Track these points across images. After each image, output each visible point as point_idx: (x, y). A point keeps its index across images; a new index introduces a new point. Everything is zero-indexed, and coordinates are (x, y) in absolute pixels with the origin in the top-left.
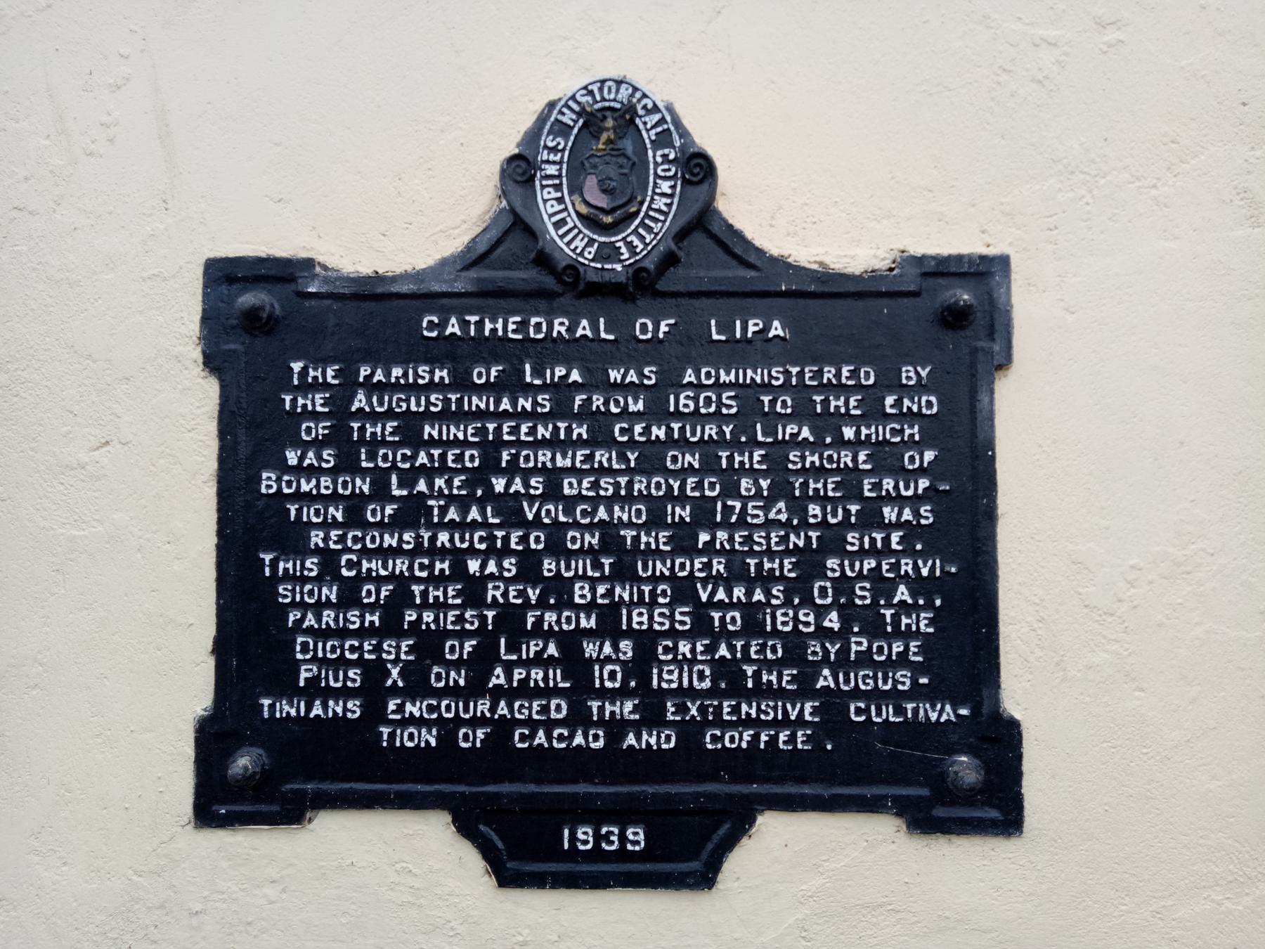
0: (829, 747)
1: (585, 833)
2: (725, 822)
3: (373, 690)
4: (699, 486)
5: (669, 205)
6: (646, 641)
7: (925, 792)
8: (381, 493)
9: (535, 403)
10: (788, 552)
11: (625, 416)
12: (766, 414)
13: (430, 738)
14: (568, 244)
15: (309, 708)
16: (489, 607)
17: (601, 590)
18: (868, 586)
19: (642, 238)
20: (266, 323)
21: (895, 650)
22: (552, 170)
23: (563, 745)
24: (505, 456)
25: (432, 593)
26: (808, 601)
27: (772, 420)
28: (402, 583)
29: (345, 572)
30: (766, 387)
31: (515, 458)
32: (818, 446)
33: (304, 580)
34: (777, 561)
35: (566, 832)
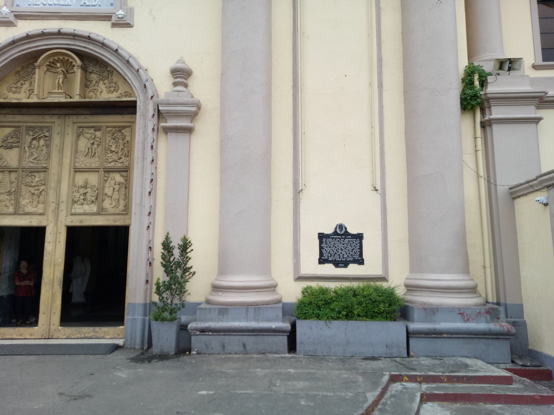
3: (328, 257)
20: (322, 237)
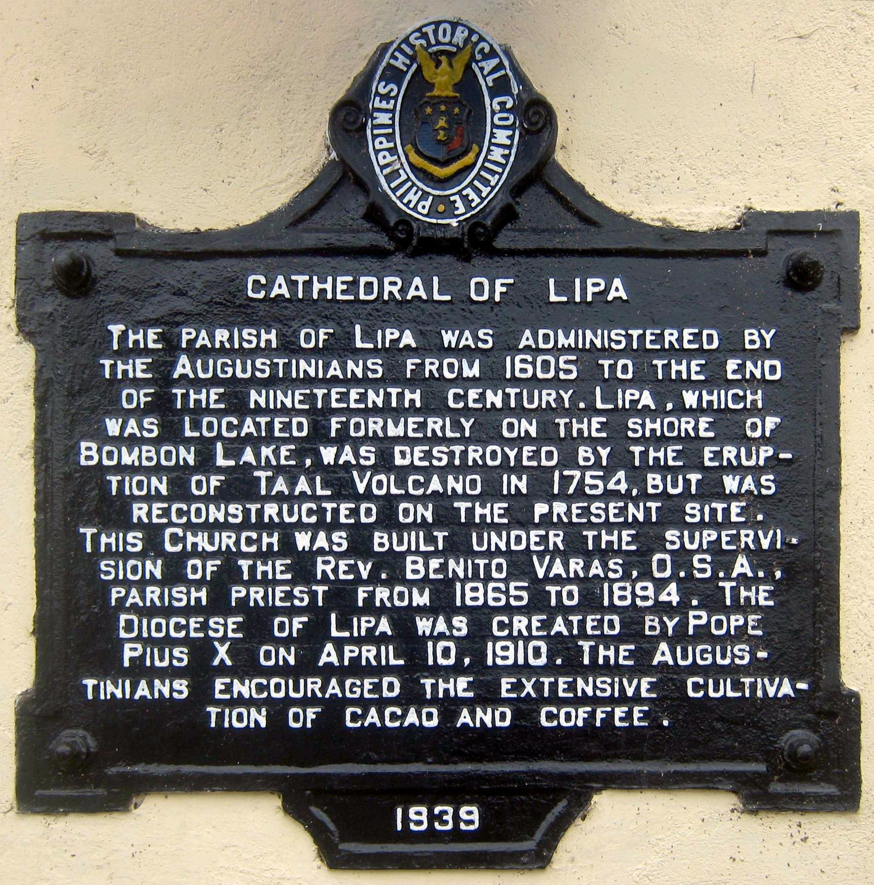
0: (666, 723)
1: (418, 814)
2: (560, 800)
3: (201, 669)
4: (536, 455)
6: (479, 618)
7: (762, 768)
9: (366, 368)
10: (626, 525)
11: (460, 382)
12: (606, 380)
15: (134, 688)
17: (434, 563)
18: (708, 558)
19: (478, 192)
21: (733, 624)
22: (383, 118)
23: (397, 724)
24: (335, 424)
25: (260, 568)
26: (645, 574)
27: (612, 385)
28: (229, 558)
31: (345, 425)
32: (659, 412)
33: (126, 556)
34: (616, 533)
35: (399, 811)
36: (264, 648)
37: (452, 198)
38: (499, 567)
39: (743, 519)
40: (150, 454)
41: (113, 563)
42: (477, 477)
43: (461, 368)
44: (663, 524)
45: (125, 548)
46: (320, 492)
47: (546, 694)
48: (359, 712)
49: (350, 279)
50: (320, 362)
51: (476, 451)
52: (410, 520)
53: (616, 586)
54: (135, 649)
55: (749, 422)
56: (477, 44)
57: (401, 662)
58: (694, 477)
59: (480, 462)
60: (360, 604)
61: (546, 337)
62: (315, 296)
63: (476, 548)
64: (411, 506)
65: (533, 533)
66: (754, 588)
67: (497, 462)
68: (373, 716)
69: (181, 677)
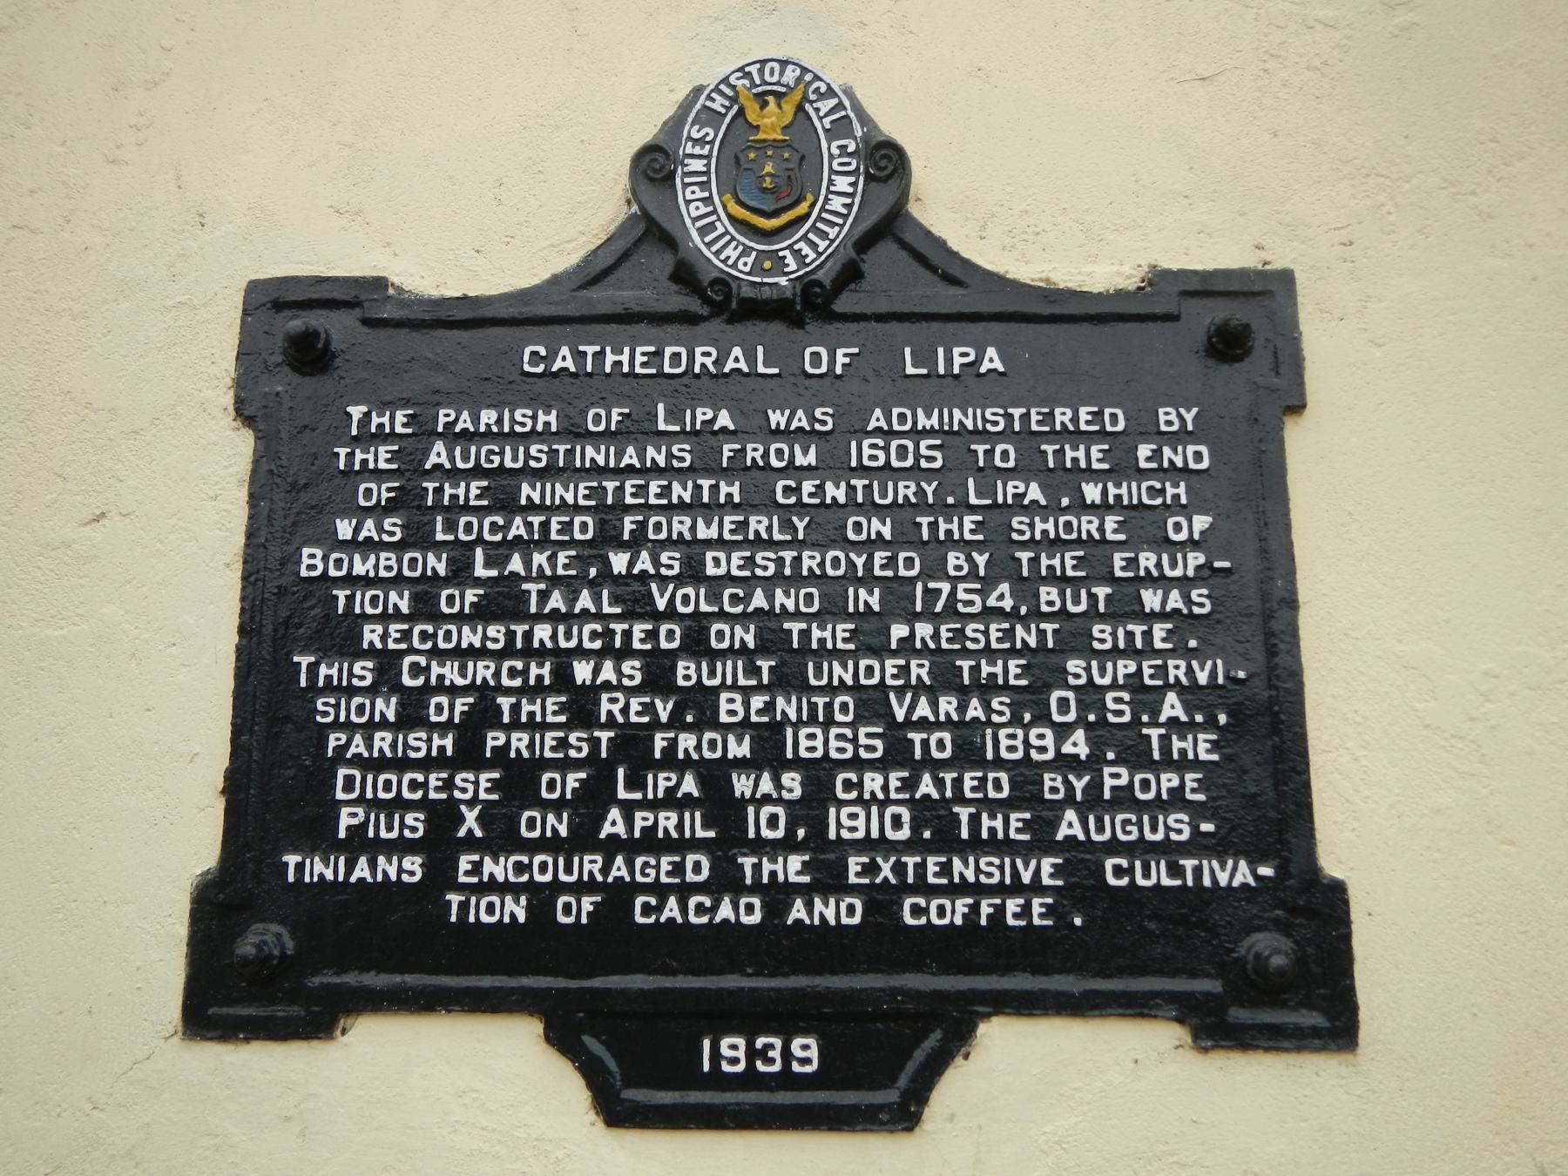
0: (1078, 921)
1: (733, 1047)
2: (933, 1031)
3: (441, 842)
4: (891, 562)
5: (849, 206)
6: (819, 773)
7: (1213, 986)
8: (460, 573)
9: (670, 456)
10: (1013, 652)
11: (791, 471)
12: (981, 470)
13: (518, 909)
14: (717, 254)
16: (603, 727)
17: (757, 702)
19: (814, 246)
20: (307, 342)
21: (1165, 785)
22: (698, 165)
23: (704, 920)
24: (628, 524)
25: (526, 708)
26: (1043, 717)
27: (989, 475)
28: (485, 693)
29: (407, 681)
30: (980, 434)
31: (642, 525)
32: (1051, 509)
33: (351, 691)
34: (1000, 663)
35: (707, 1044)
36: (527, 814)
37: (781, 254)
38: (844, 708)
39: (1170, 646)
40: (389, 563)
41: (332, 701)
42: (814, 591)
43: (792, 455)
44: (1062, 651)
45: (349, 681)
46: (607, 609)
47: (910, 880)
48: (653, 901)
49: (652, 349)
50: (612, 449)
51: (813, 557)
52: (725, 645)
53: (1002, 733)
54: (355, 815)
55: (1171, 522)
56: (810, 83)
57: (711, 834)
58: (1102, 592)
59: (818, 572)
60: (658, 755)
61: (902, 417)
62: (608, 369)
63: (813, 682)
64: (726, 628)
65: (889, 663)
66: (1190, 737)
67: (841, 572)
68: (672, 909)
69: (414, 853)
